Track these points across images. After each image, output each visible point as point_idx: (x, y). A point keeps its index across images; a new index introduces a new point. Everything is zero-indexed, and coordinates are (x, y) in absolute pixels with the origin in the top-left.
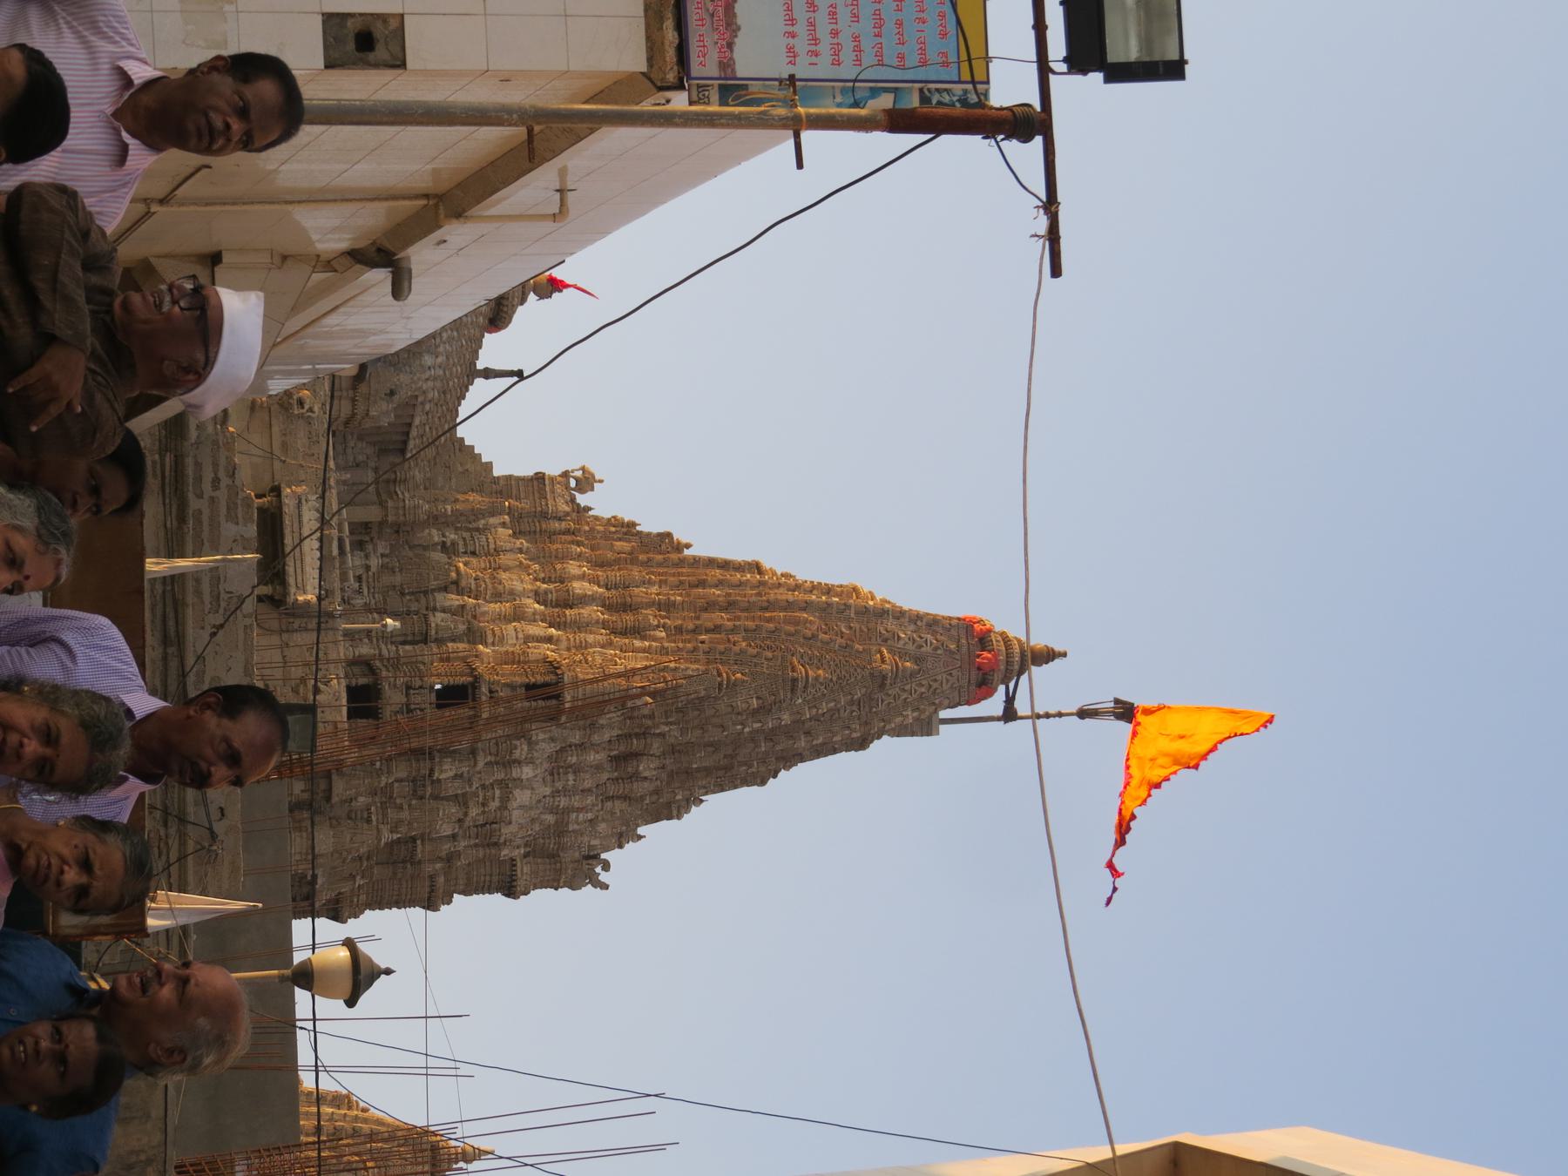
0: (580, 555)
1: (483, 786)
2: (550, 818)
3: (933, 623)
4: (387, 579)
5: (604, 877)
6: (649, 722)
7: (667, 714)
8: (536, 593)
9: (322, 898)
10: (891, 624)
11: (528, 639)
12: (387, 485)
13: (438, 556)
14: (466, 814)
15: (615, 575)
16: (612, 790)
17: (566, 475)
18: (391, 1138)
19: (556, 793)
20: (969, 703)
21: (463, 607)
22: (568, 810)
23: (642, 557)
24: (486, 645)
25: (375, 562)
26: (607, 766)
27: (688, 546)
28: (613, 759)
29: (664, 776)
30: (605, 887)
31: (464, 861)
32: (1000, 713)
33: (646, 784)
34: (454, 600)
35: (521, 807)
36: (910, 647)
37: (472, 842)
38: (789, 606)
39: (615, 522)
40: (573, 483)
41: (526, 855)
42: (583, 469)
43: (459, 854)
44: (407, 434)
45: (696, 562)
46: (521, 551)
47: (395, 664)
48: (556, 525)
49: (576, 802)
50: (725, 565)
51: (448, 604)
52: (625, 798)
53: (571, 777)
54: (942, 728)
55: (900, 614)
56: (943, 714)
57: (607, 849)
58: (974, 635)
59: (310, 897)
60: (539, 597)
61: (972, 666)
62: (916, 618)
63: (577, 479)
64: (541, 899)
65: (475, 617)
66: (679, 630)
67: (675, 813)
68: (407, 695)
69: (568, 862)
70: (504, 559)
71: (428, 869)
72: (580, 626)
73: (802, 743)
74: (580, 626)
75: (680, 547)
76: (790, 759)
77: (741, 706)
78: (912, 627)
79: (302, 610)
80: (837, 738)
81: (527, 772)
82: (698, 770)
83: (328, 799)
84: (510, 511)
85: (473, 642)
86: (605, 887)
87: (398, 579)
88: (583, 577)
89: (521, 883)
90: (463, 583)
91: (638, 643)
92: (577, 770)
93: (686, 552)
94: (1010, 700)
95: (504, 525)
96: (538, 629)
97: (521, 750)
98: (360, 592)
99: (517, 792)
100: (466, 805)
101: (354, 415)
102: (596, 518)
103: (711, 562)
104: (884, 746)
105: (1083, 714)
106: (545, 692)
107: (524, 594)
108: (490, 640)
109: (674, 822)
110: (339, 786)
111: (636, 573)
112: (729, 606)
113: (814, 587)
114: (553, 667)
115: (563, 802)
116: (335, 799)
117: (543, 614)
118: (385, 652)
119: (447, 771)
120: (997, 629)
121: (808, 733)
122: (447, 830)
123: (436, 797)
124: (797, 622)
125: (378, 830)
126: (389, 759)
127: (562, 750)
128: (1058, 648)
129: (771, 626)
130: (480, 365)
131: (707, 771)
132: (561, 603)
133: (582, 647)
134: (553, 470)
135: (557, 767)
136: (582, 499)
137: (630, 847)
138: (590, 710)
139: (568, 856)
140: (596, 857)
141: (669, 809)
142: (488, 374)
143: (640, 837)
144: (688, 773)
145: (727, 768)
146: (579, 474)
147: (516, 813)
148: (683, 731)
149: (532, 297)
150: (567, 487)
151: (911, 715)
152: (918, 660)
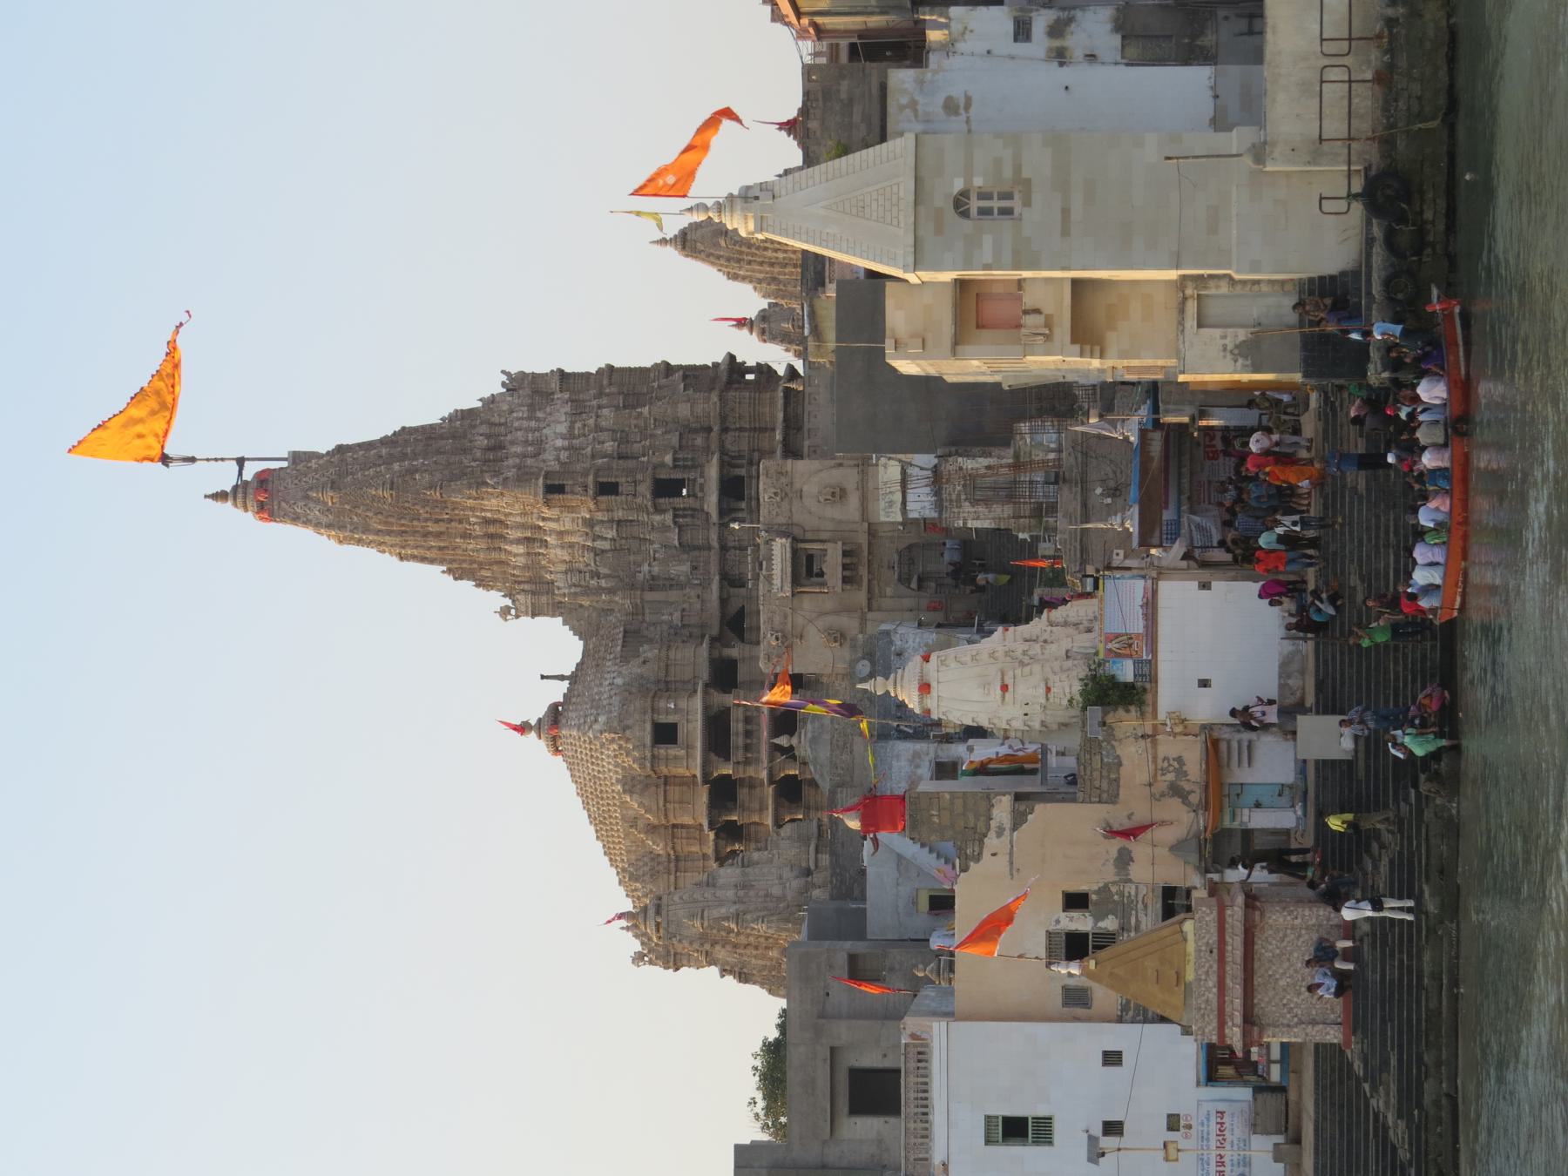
2: (540, 414)
3: (295, 519)
4: (639, 558)
5: (504, 378)
9: (678, 375)
10: (324, 520)
11: (557, 520)
12: (638, 611)
13: (604, 571)
15: (494, 555)
17: (517, 617)
18: (709, 255)
19: (538, 429)
22: (529, 418)
24: (584, 519)
25: (646, 568)
34: (599, 544)
36: (312, 505)
38: (389, 533)
45: (441, 562)
47: (640, 509)
48: (526, 587)
49: (525, 424)
50: (423, 559)
52: (493, 424)
55: (317, 526)
56: (285, 464)
59: (685, 377)
60: (545, 544)
61: (270, 492)
62: (307, 523)
64: (541, 364)
66: (460, 522)
69: (529, 390)
70: (563, 567)
71: (614, 389)
72: (523, 526)
74: (523, 526)
75: (449, 571)
76: (384, 441)
77: (426, 475)
79: (784, 534)
81: (559, 443)
85: (591, 519)
87: (632, 558)
88: (516, 555)
89: (557, 377)
97: (564, 455)
103: (432, 561)
104: (324, 446)
105: (193, 460)
106: (554, 489)
107: (555, 547)
110: (675, 440)
111: (482, 556)
112: (426, 535)
113: (369, 544)
114: (547, 503)
115: (533, 424)
119: (609, 446)
120: (250, 514)
122: (605, 412)
124: (386, 523)
127: (536, 455)
130: (566, 684)
131: (442, 437)
133: (524, 514)
134: (526, 620)
135: (540, 444)
136: (508, 602)
137: (487, 395)
138: (523, 477)
139: (528, 391)
142: (562, 678)
144: (454, 437)
149: (533, 722)
151: (313, 464)
152: (307, 497)
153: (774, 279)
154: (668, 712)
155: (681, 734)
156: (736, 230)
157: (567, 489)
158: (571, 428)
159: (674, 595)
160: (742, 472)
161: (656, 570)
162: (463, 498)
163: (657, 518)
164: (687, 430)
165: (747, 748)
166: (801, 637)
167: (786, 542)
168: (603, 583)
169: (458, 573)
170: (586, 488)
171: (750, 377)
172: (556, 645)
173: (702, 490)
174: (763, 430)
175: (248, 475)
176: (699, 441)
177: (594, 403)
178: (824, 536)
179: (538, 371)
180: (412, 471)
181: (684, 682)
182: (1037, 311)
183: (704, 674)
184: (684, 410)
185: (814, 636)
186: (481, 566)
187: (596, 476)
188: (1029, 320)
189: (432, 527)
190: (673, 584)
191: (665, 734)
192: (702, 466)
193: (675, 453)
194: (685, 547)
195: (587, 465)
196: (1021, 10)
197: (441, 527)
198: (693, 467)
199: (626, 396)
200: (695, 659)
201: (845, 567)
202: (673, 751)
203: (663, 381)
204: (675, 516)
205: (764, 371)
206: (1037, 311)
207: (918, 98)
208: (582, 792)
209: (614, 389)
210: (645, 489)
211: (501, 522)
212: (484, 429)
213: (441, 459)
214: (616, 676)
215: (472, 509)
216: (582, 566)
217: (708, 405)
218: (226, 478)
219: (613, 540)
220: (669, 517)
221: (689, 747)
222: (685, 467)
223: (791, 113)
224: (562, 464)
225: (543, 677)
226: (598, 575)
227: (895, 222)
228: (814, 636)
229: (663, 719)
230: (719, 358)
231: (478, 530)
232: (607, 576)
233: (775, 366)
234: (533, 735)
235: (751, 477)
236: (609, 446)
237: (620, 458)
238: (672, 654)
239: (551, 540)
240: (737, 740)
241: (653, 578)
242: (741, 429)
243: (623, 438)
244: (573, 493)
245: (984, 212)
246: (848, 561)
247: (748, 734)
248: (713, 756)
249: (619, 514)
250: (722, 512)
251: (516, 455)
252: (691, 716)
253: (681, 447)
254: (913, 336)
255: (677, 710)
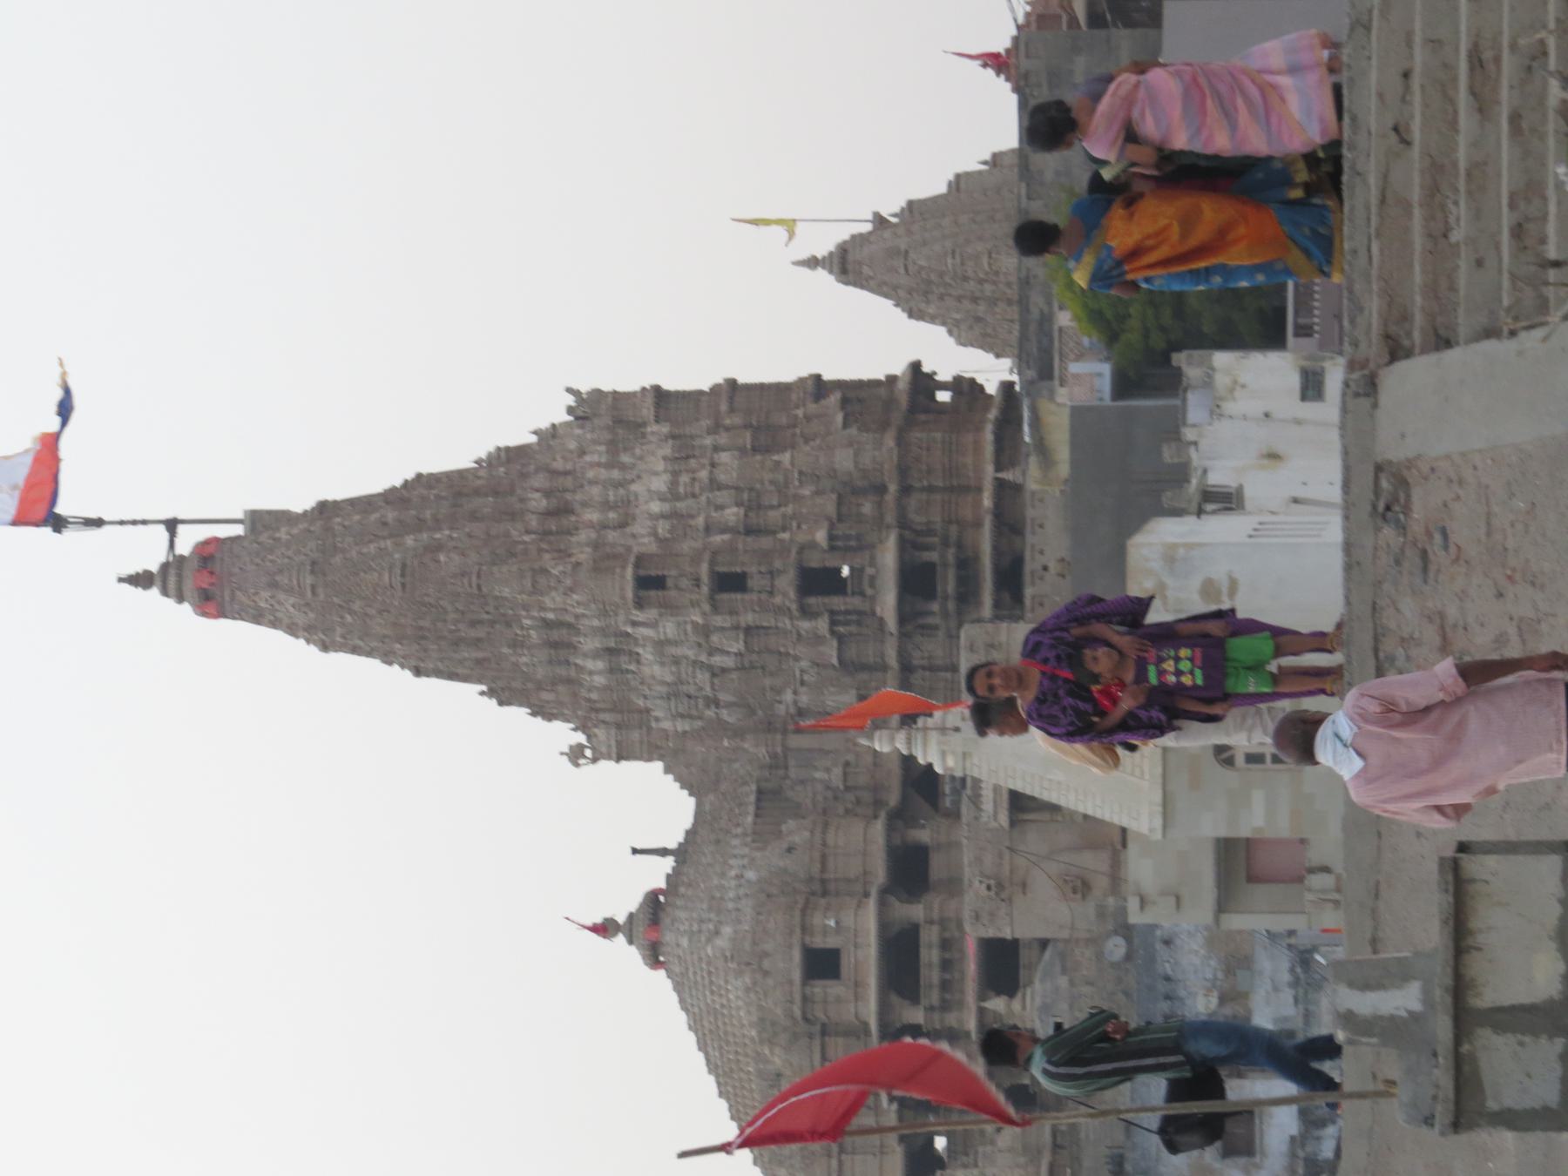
0: (589, 691)
1: (694, 496)
2: (625, 458)
3: (257, 618)
6: (544, 546)
7: (526, 552)
8: (638, 662)
9: (834, 398)
10: (301, 619)
11: (653, 625)
12: (777, 763)
13: (724, 697)
14: (711, 472)
15: (562, 671)
16: (568, 482)
17: (594, 760)
20: (216, 540)
21: (710, 655)
22: (609, 466)
23: (530, 685)
25: (788, 696)
26: (577, 507)
27: (482, 693)
28: (572, 512)
29: (519, 491)
30: (569, 390)
31: (706, 423)
32: (181, 529)
33: (536, 485)
34: (718, 660)
35: (656, 474)
36: (282, 596)
37: (697, 442)
39: (549, 717)
40: (588, 753)
41: (644, 424)
42: (577, 765)
43: (710, 431)
44: (758, 808)
45: (479, 681)
46: (645, 697)
47: (780, 611)
49: (603, 474)
50: (452, 676)
51: (725, 658)
52: (554, 473)
53: (611, 498)
54: (240, 516)
55: (292, 630)
56: (238, 530)
57: (567, 424)
58: (211, 603)
59: (845, 402)
62: (274, 624)
63: (585, 757)
64: (629, 383)
65: (699, 645)
66: (508, 625)
67: (503, 454)
68: (772, 586)
70: (663, 690)
71: (737, 420)
74: (603, 632)
75: (491, 693)
76: (394, 497)
78: (279, 615)
80: (357, 517)
81: (656, 507)
82: (486, 495)
83: (840, 498)
84: (649, 728)
86: (569, 390)
87: (768, 682)
88: (591, 673)
90: (707, 675)
91: (551, 616)
92: (606, 506)
93: (484, 688)
95: (657, 719)
97: (663, 528)
98: (802, 671)
99: (664, 488)
100: (712, 480)
101: (824, 832)
102: (568, 721)
104: (300, 502)
105: (98, 523)
108: (689, 628)
109: (502, 444)
110: (831, 509)
111: (541, 673)
112: (456, 643)
115: (616, 474)
116: (834, 496)
117: (637, 644)
118: (787, 621)
119: (732, 514)
121: (385, 524)
122: (724, 457)
123: (737, 488)
125: (792, 464)
126: (784, 529)
127: (622, 525)
128: (126, 586)
129: (421, 623)
131: (477, 492)
132: (617, 651)
134: (606, 765)
136: (580, 738)
137: (544, 424)
138: (606, 559)
139: (607, 420)
140: (577, 418)
141: (510, 457)
142: (663, 852)
143: (535, 433)
144: (496, 493)
145: (459, 494)
146: (582, 761)
147: (660, 466)
148: (507, 535)
149: (621, 919)
150: (593, 749)
151: (283, 534)
153: (978, 319)
154: (825, 930)
156: (930, 766)
157: (670, 583)
158: (674, 483)
159: (832, 741)
160: (933, 556)
161: (804, 699)
163: (805, 625)
164: (849, 492)
165: (945, 986)
166: (1024, 885)
168: (724, 714)
169: (504, 694)
170: (697, 582)
171: (943, 396)
172: (651, 805)
173: (872, 585)
174: (965, 489)
175: (184, 546)
176: (867, 508)
177: (708, 441)
179: (622, 388)
181: (848, 881)
182: (1326, 869)
183: (880, 875)
184: (844, 460)
185: (1043, 887)
186: (540, 687)
187: (712, 563)
188: (1317, 881)
189: (467, 632)
190: (827, 723)
191: (822, 964)
192: (872, 547)
193: (832, 526)
194: (848, 666)
195: (698, 544)
196: (1310, 358)
197: (480, 632)
198: (860, 548)
199: (756, 430)
200: (865, 845)
202: (834, 989)
203: (812, 407)
204: (833, 623)
205: (966, 388)
206: (1326, 869)
207: (1169, 581)
208: (696, 1025)
209: (737, 420)
210: (787, 584)
211: (570, 626)
212: (540, 481)
213: (477, 528)
214: (743, 868)
215: (526, 607)
216: (692, 690)
217: (881, 451)
218: (150, 552)
219: (739, 654)
220: (822, 625)
221: (858, 984)
222: (848, 549)
223: (1000, 41)
224: (661, 541)
225: (635, 851)
226: (717, 703)
227: (1137, 772)
228: (1043, 887)
229: (818, 942)
230: (898, 368)
232: (729, 705)
233: (980, 380)
234: (621, 939)
235: (945, 565)
236: (732, 514)
237: (750, 531)
238: (831, 840)
239: (647, 654)
240: (930, 973)
241: (801, 713)
242: (931, 489)
243: (754, 505)
244: (677, 587)
245: (1254, 759)
247: (946, 965)
248: (895, 999)
249: (749, 618)
250: (903, 619)
251: (591, 525)
252: (859, 932)
253: (840, 518)
254: (1163, 893)
255: (839, 928)
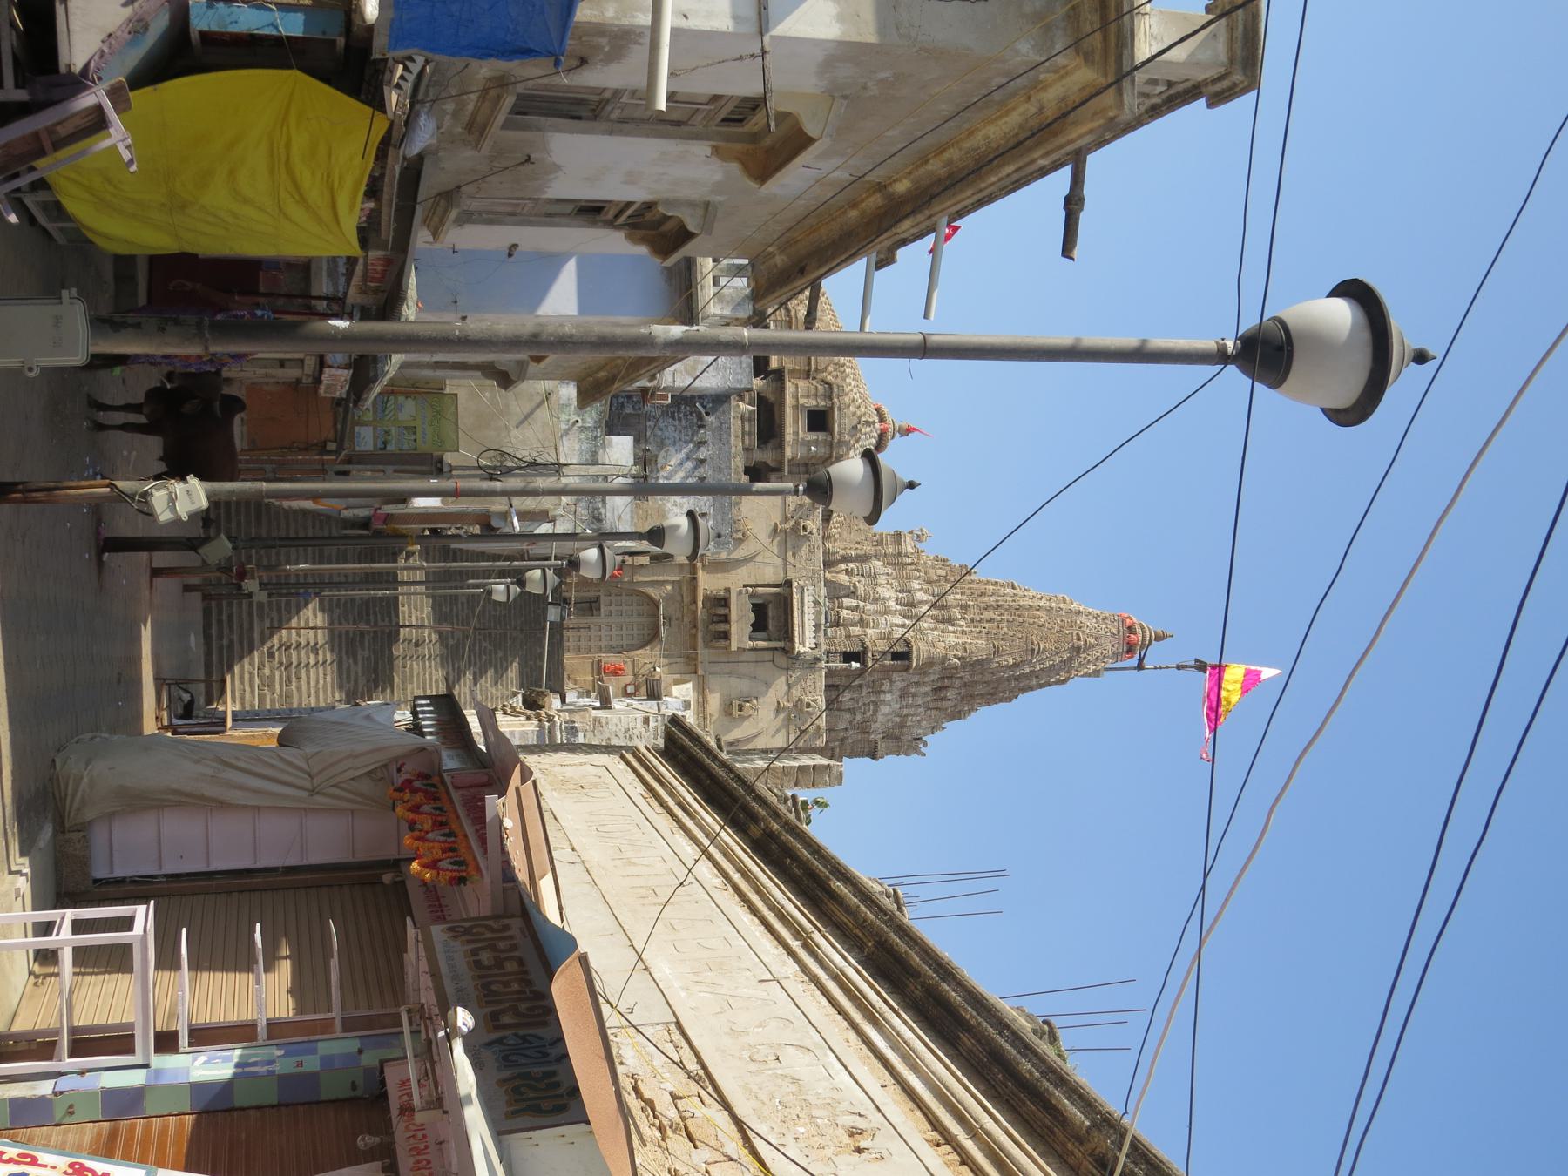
5: (923, 749)
60: (898, 601)
64: (890, 761)
73: (1034, 682)
81: (888, 697)
92: (914, 695)
94: (1141, 660)
96: (899, 621)
105: (1179, 667)
115: (905, 711)
119: (847, 696)
135: (904, 694)
137: (938, 733)
139: (906, 738)
141: (956, 715)
154: (816, 443)
155: (803, 422)
157: (889, 656)
158: (875, 712)
162: (979, 646)
166: (775, 530)
167: (798, 648)
178: (752, 656)
180: (1016, 665)
191: (819, 420)
197: (989, 614)
201: (726, 619)
202: (811, 403)
213: (988, 677)
215: (963, 632)
221: (796, 407)
229: (821, 436)
231: (956, 612)
246: (722, 627)
248: (771, 398)
